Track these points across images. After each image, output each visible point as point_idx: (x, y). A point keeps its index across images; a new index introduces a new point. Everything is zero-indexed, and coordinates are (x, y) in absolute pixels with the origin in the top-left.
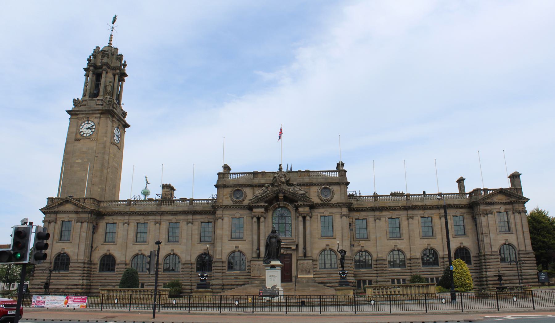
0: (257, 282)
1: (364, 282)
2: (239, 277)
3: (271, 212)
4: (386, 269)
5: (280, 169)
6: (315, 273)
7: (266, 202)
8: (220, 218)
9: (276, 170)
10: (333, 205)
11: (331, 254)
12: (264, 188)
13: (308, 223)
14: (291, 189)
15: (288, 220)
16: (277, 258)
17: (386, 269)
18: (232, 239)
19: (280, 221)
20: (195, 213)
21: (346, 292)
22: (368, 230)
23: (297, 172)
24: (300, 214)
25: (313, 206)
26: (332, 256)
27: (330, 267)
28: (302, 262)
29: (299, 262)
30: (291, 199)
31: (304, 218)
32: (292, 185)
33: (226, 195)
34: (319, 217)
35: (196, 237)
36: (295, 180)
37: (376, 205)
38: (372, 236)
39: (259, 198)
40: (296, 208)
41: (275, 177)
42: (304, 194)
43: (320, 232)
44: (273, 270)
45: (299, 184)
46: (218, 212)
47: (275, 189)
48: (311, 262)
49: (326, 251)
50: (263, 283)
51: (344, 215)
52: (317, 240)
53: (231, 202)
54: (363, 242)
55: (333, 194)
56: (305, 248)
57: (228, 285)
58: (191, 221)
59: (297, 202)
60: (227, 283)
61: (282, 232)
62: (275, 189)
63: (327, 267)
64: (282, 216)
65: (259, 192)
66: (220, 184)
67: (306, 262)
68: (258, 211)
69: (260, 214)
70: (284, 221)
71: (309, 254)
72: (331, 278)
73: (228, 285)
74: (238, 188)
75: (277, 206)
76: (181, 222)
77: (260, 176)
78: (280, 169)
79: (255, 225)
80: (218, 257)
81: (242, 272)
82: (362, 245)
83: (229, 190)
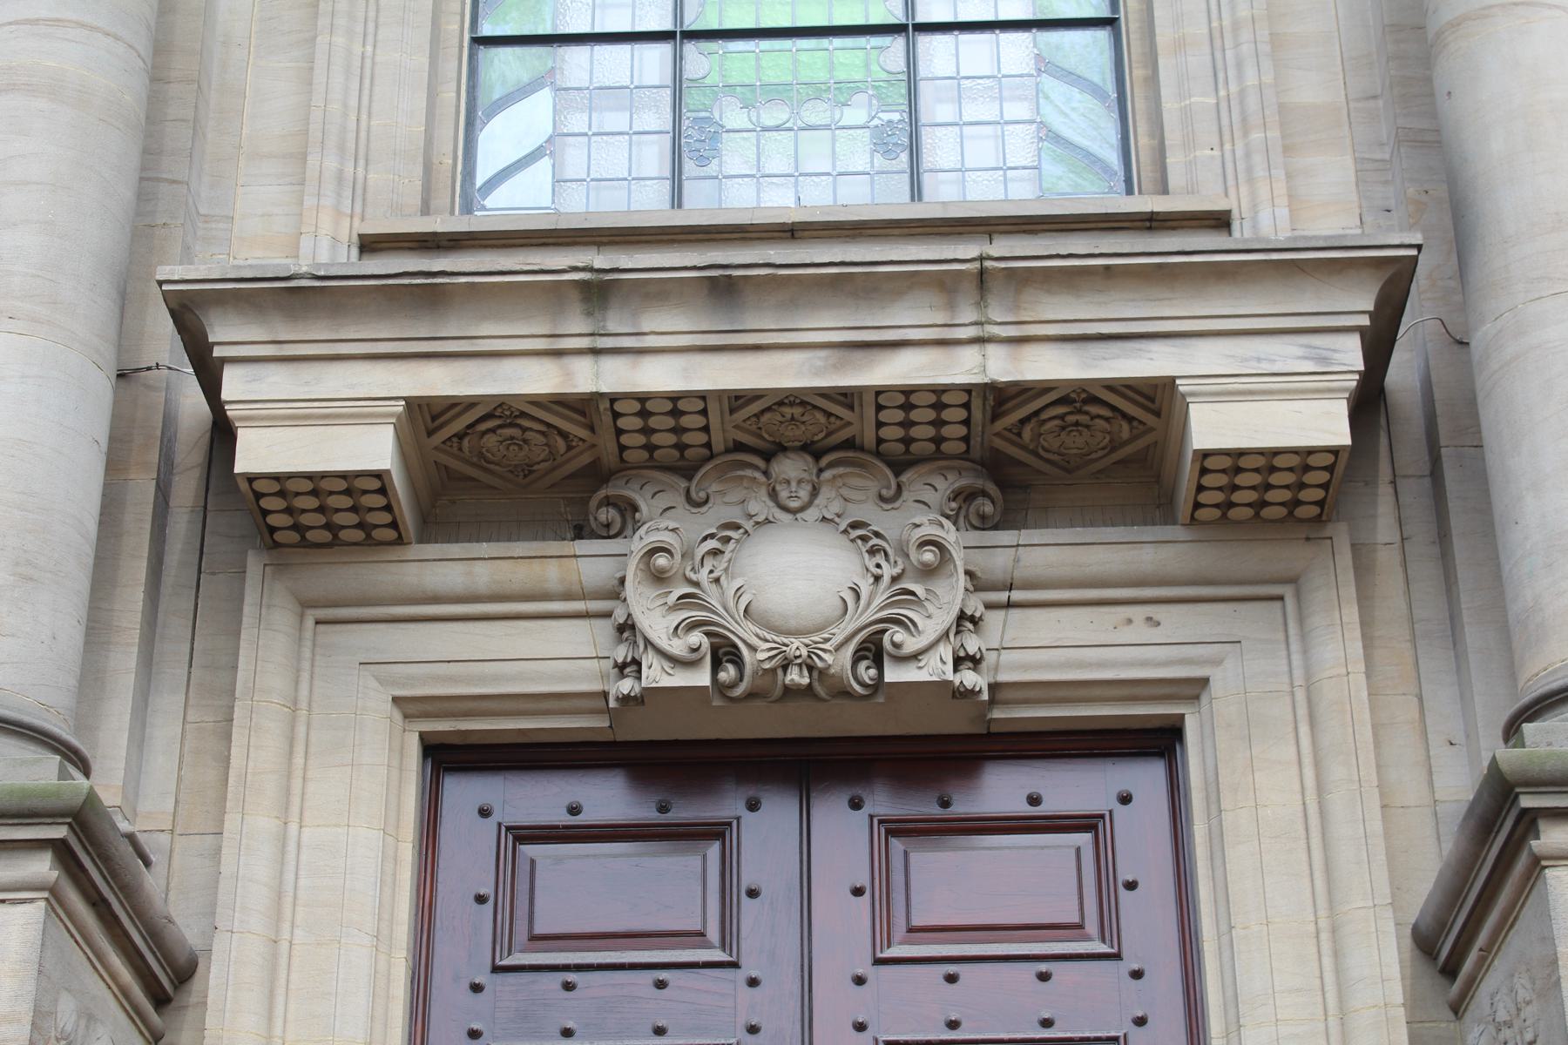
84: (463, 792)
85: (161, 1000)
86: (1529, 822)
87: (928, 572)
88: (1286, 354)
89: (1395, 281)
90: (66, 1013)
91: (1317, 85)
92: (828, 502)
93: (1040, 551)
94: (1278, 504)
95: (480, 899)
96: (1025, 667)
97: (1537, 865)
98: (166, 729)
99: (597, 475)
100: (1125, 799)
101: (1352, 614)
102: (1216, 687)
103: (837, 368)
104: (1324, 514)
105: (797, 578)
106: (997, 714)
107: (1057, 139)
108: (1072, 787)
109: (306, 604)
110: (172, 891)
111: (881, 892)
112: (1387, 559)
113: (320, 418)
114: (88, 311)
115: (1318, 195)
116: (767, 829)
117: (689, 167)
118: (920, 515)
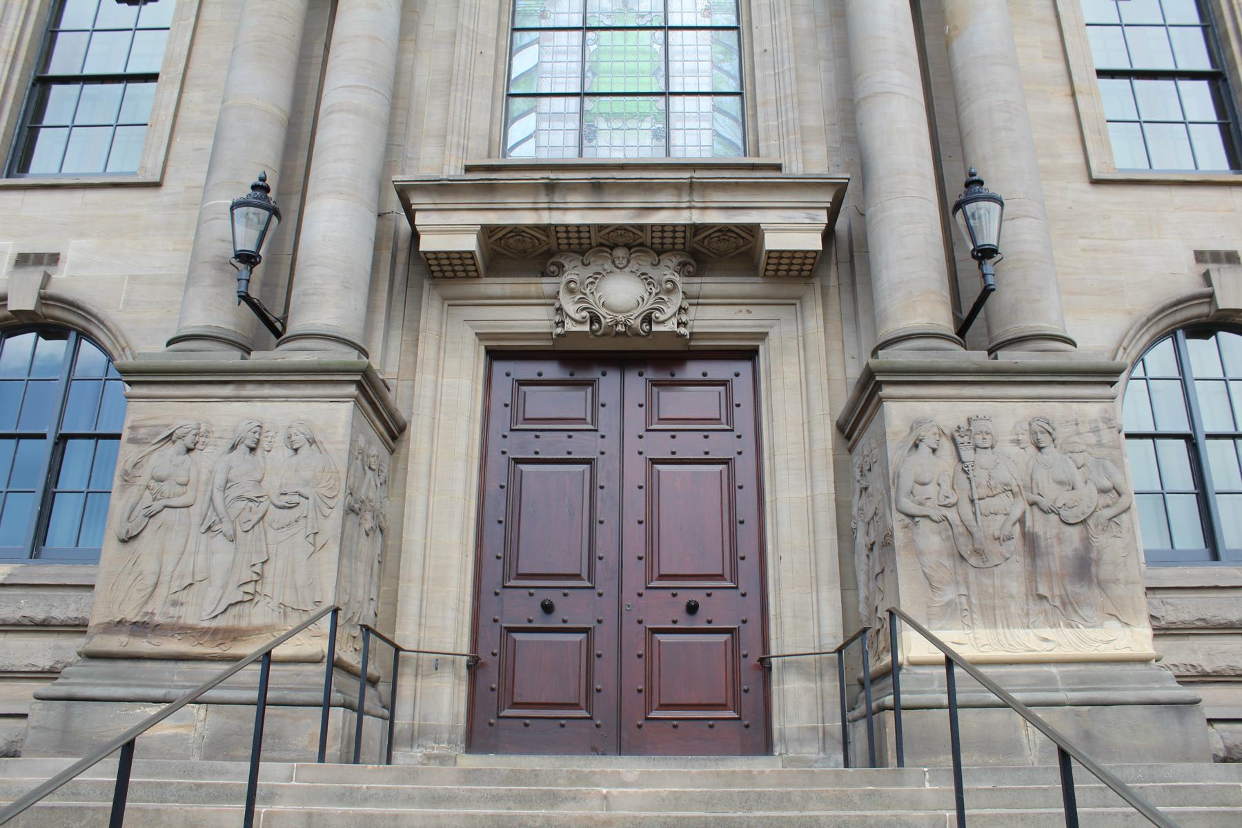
28: (944, 411)
29: (899, 413)
67: (1008, 414)
84: (500, 367)
85: (394, 438)
86: (879, 385)
87: (669, 292)
88: (800, 216)
89: (840, 191)
90: (362, 441)
91: (815, 119)
92: (633, 266)
93: (710, 285)
94: (795, 271)
95: (506, 405)
96: (703, 327)
97: (881, 400)
98: (395, 343)
99: (550, 254)
100: (737, 375)
101: (820, 311)
102: (771, 335)
103: (638, 216)
104: (812, 274)
105: (621, 293)
106: (692, 343)
107: (719, 135)
108: (718, 370)
109: (445, 299)
110: (398, 399)
111: (649, 406)
112: (833, 292)
113: (451, 232)
114: (367, 191)
115: (813, 159)
116: (609, 383)
117: (585, 142)
118: (667, 271)
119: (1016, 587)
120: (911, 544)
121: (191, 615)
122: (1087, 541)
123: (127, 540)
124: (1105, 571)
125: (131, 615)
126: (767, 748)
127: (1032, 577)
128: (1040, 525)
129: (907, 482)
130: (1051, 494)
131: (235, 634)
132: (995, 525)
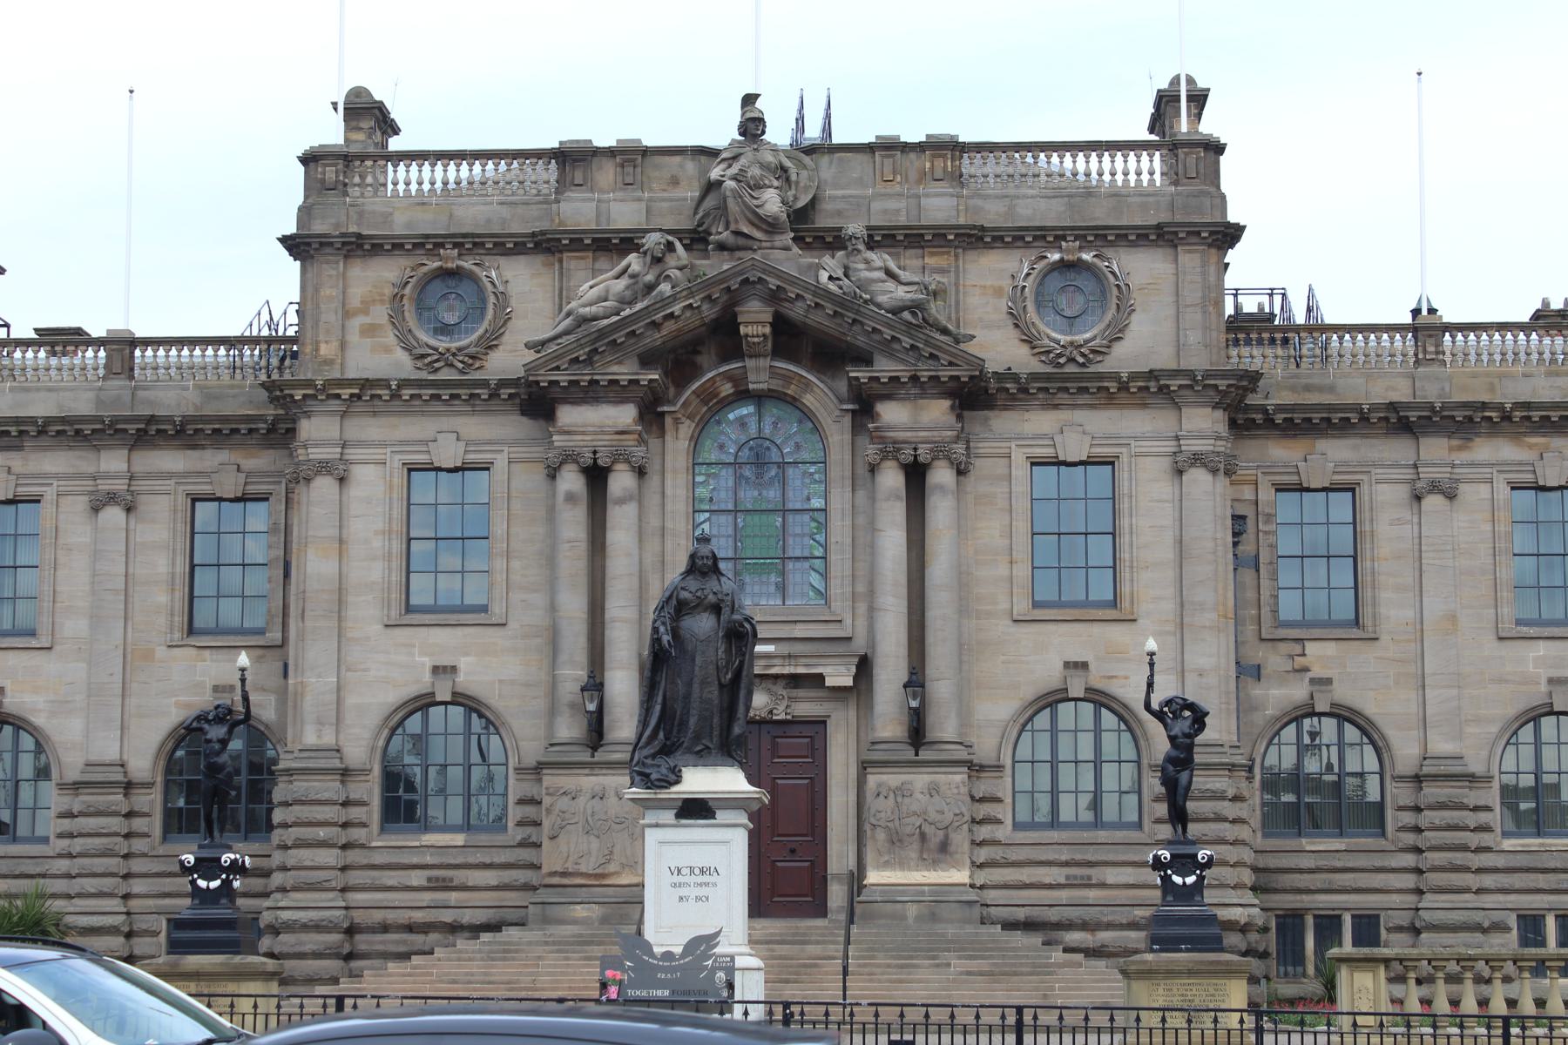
0: (580, 911)
1: (1328, 927)
2: (460, 876)
3: (687, 428)
4: (1486, 839)
5: (752, 127)
6: (983, 854)
7: (646, 361)
8: (324, 467)
9: (722, 132)
10: (1124, 387)
11: (1098, 731)
12: (634, 261)
13: (940, 511)
14: (828, 268)
15: (801, 489)
16: (727, 749)
17: (1486, 839)
18: (410, 612)
19: (748, 496)
20: (148, 432)
21: (1197, 992)
22: (1365, 565)
23: (869, 149)
24: (890, 449)
25: (975, 394)
26: (1109, 740)
27: (1087, 816)
28: (892, 779)
29: (872, 780)
30: (817, 342)
31: (916, 475)
32: (833, 241)
33: (366, 312)
34: (1020, 469)
35: (159, 601)
36: (853, 203)
37: (1431, 393)
38: (1392, 610)
39: (602, 334)
40: (863, 406)
41: (712, 187)
42: (914, 307)
43: (1023, 571)
44: (696, 831)
45: (883, 238)
46: (308, 428)
47: (715, 266)
48: (959, 777)
49: (1066, 709)
50: (624, 919)
51: (1197, 459)
52: (1003, 626)
53: (402, 356)
54: (1330, 649)
55: (1125, 309)
56: (916, 681)
57: (385, 928)
58: (120, 486)
59: (865, 360)
60: (378, 916)
61: (761, 569)
62: (715, 266)
63: (1066, 815)
64: (760, 463)
65: (597, 288)
66: (319, 227)
67: (920, 780)
68: (595, 423)
69: (604, 443)
70: (773, 494)
71: (943, 726)
72: (1092, 895)
73: (385, 928)
74: (451, 258)
75: (727, 389)
76: (49, 493)
77: (606, 174)
78: (752, 127)
79: (573, 524)
80: (310, 738)
81: (483, 839)
82: (1318, 671)
83: (385, 273)
88: (842, 669)
93: (801, 693)
111: (774, 751)
119: (914, 855)
120: (873, 837)
121: (583, 869)
122: (947, 837)
123: (553, 838)
124: (952, 848)
125: (560, 869)
126: (825, 915)
127: (921, 852)
128: (927, 829)
129: (873, 811)
130: (933, 816)
131: (603, 876)
132: (908, 830)
